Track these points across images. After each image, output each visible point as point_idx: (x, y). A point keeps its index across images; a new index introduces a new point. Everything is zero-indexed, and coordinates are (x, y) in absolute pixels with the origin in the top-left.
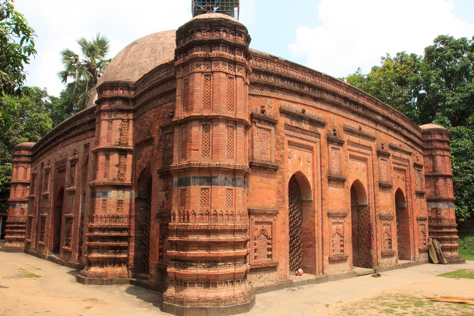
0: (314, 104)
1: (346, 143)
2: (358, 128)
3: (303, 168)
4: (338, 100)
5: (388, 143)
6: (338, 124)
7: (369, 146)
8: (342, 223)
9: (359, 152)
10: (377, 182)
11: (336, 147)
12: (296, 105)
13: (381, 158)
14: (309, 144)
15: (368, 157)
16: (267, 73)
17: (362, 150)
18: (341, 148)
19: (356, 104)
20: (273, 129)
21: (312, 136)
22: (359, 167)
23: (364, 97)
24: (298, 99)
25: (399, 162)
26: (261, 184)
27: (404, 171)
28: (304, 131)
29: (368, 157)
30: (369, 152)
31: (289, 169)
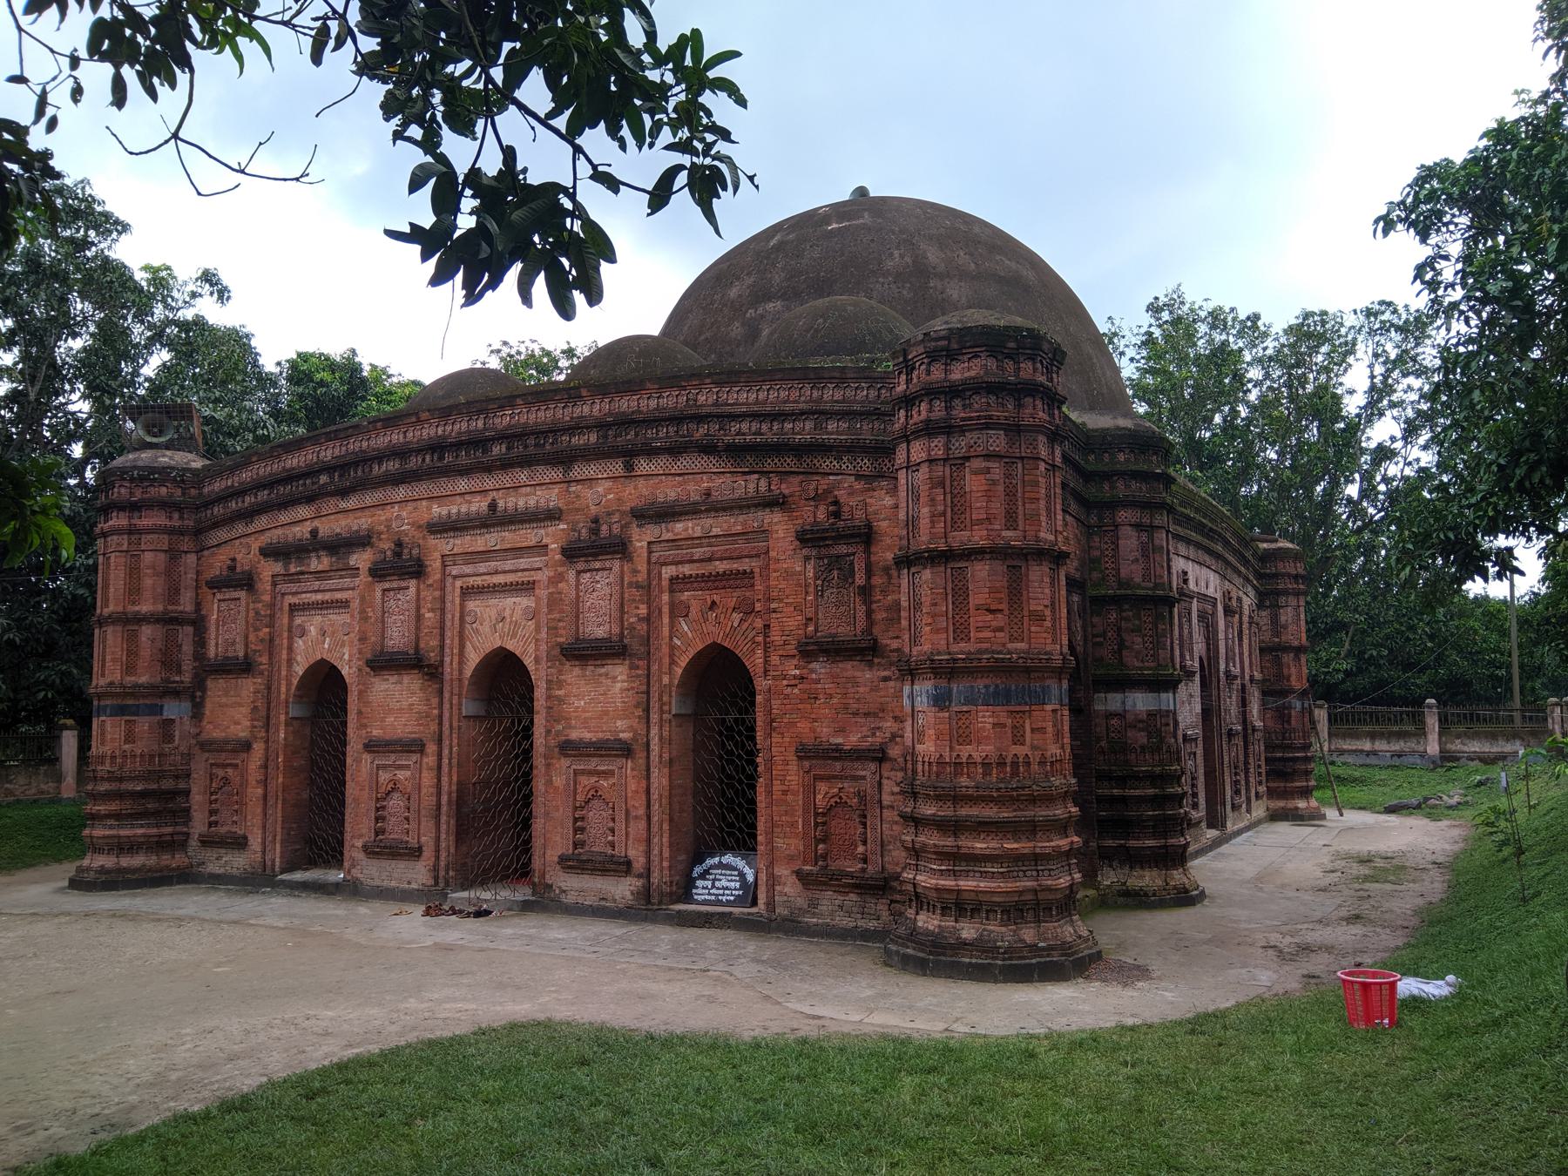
0: (343, 505)
1: (434, 564)
2: (484, 505)
3: (330, 650)
4: (414, 462)
5: (627, 507)
6: (413, 524)
7: (532, 543)
8: (407, 767)
9: (496, 572)
10: (560, 644)
11: (395, 584)
12: (297, 524)
13: (581, 566)
14: (338, 596)
15: (537, 576)
16: (240, 493)
17: (509, 565)
18: (413, 583)
19: (478, 442)
20: (242, 594)
21: (341, 577)
22: (507, 613)
23: (513, 406)
24: (303, 511)
25: (698, 553)
26: (224, 700)
27: (747, 575)
28: (320, 575)
29: (537, 576)
30: (537, 561)
31: (299, 658)
